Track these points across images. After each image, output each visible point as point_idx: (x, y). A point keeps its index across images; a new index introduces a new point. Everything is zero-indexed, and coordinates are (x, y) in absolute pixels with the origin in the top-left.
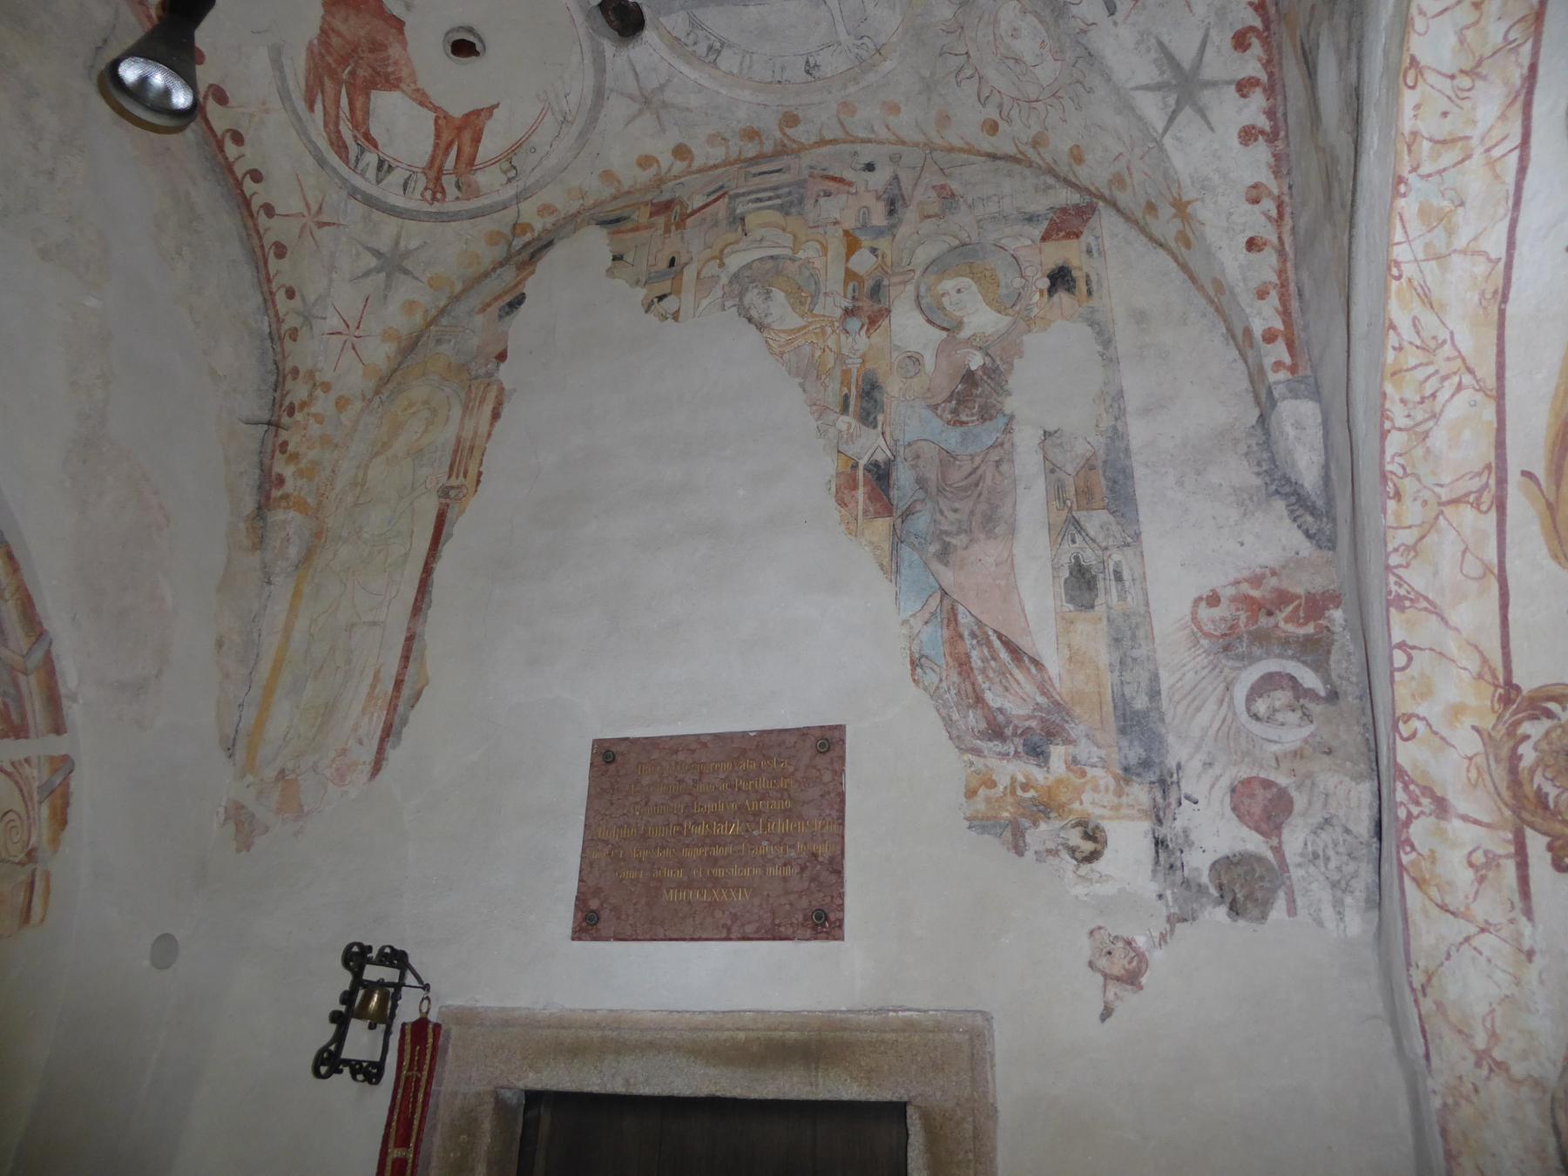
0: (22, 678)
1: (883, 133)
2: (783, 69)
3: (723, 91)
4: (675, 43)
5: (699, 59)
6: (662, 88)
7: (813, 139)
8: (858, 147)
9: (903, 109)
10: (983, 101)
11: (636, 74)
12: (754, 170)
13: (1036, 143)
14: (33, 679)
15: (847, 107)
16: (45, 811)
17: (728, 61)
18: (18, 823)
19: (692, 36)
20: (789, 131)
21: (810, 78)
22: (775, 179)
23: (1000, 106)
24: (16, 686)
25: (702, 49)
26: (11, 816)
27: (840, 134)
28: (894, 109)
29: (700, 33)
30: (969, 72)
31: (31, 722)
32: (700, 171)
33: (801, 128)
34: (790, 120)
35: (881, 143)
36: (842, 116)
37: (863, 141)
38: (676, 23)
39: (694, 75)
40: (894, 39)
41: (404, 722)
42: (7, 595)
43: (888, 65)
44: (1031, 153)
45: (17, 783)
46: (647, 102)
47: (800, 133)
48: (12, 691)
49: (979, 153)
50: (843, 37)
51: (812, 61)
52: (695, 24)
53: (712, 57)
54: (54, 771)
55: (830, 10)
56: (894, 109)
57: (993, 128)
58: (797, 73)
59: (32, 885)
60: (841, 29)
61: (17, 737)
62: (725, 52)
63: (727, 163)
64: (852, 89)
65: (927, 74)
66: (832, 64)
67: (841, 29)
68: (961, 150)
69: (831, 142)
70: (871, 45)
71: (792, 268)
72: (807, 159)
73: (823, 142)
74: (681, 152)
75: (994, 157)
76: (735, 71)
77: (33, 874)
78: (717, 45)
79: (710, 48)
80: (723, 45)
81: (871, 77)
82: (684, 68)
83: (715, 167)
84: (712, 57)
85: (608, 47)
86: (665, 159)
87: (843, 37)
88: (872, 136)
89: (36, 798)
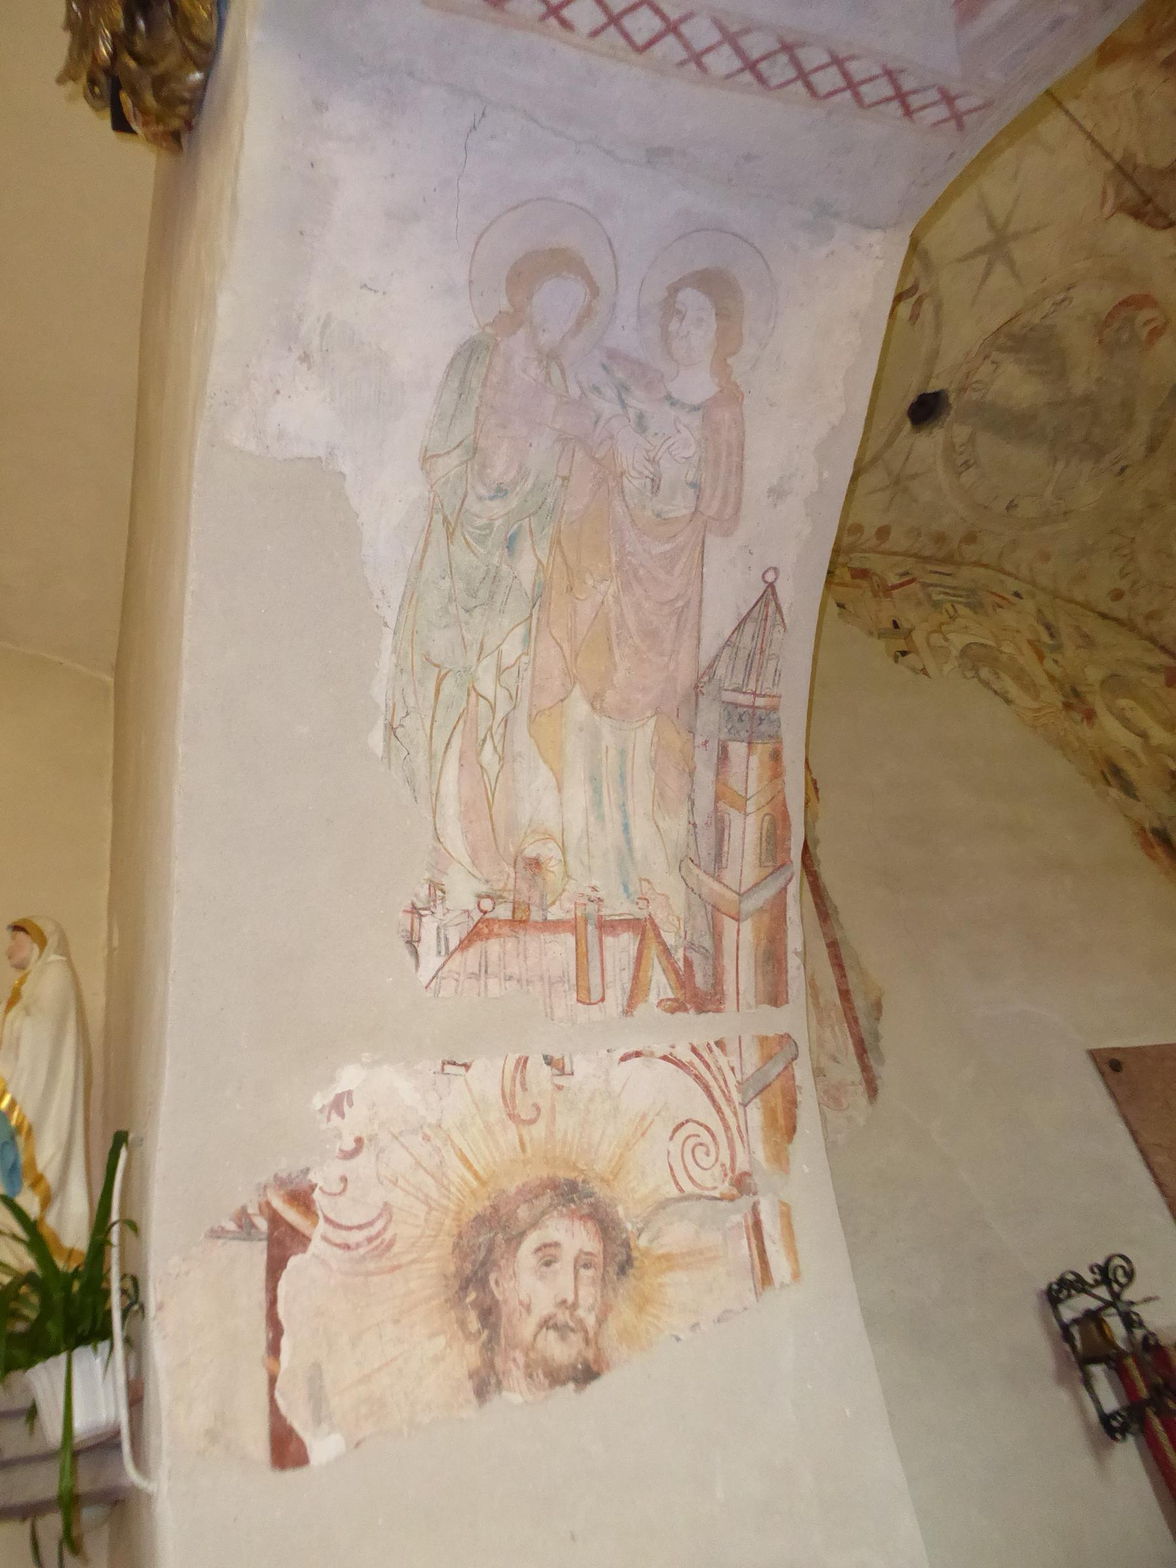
0: (729, 925)
4: (950, 447)
6: (913, 477)
7: (974, 559)
8: (1003, 577)
10: (1123, 574)
11: (907, 458)
12: (929, 567)
13: (1150, 616)
14: (747, 927)
16: (755, 1115)
17: (968, 478)
18: (706, 1137)
22: (948, 581)
23: (1134, 583)
24: (717, 935)
26: (690, 1128)
30: (1126, 551)
31: (729, 987)
32: (883, 553)
34: (971, 538)
37: (1009, 574)
38: (961, 433)
41: (877, 1037)
42: (751, 807)
44: (1140, 621)
45: (698, 1078)
46: (897, 482)
47: (970, 552)
48: (707, 942)
49: (1092, 610)
52: (971, 440)
54: (768, 1058)
56: (1045, 557)
57: (1118, 595)
59: (757, 1225)
61: (701, 1010)
63: (906, 554)
68: (1078, 603)
69: (985, 566)
71: (1004, 658)
72: (966, 572)
73: (978, 564)
74: (883, 532)
75: (1104, 616)
77: (755, 1210)
79: (966, 462)
83: (895, 554)
85: (908, 425)
86: (870, 532)
89: (736, 1097)
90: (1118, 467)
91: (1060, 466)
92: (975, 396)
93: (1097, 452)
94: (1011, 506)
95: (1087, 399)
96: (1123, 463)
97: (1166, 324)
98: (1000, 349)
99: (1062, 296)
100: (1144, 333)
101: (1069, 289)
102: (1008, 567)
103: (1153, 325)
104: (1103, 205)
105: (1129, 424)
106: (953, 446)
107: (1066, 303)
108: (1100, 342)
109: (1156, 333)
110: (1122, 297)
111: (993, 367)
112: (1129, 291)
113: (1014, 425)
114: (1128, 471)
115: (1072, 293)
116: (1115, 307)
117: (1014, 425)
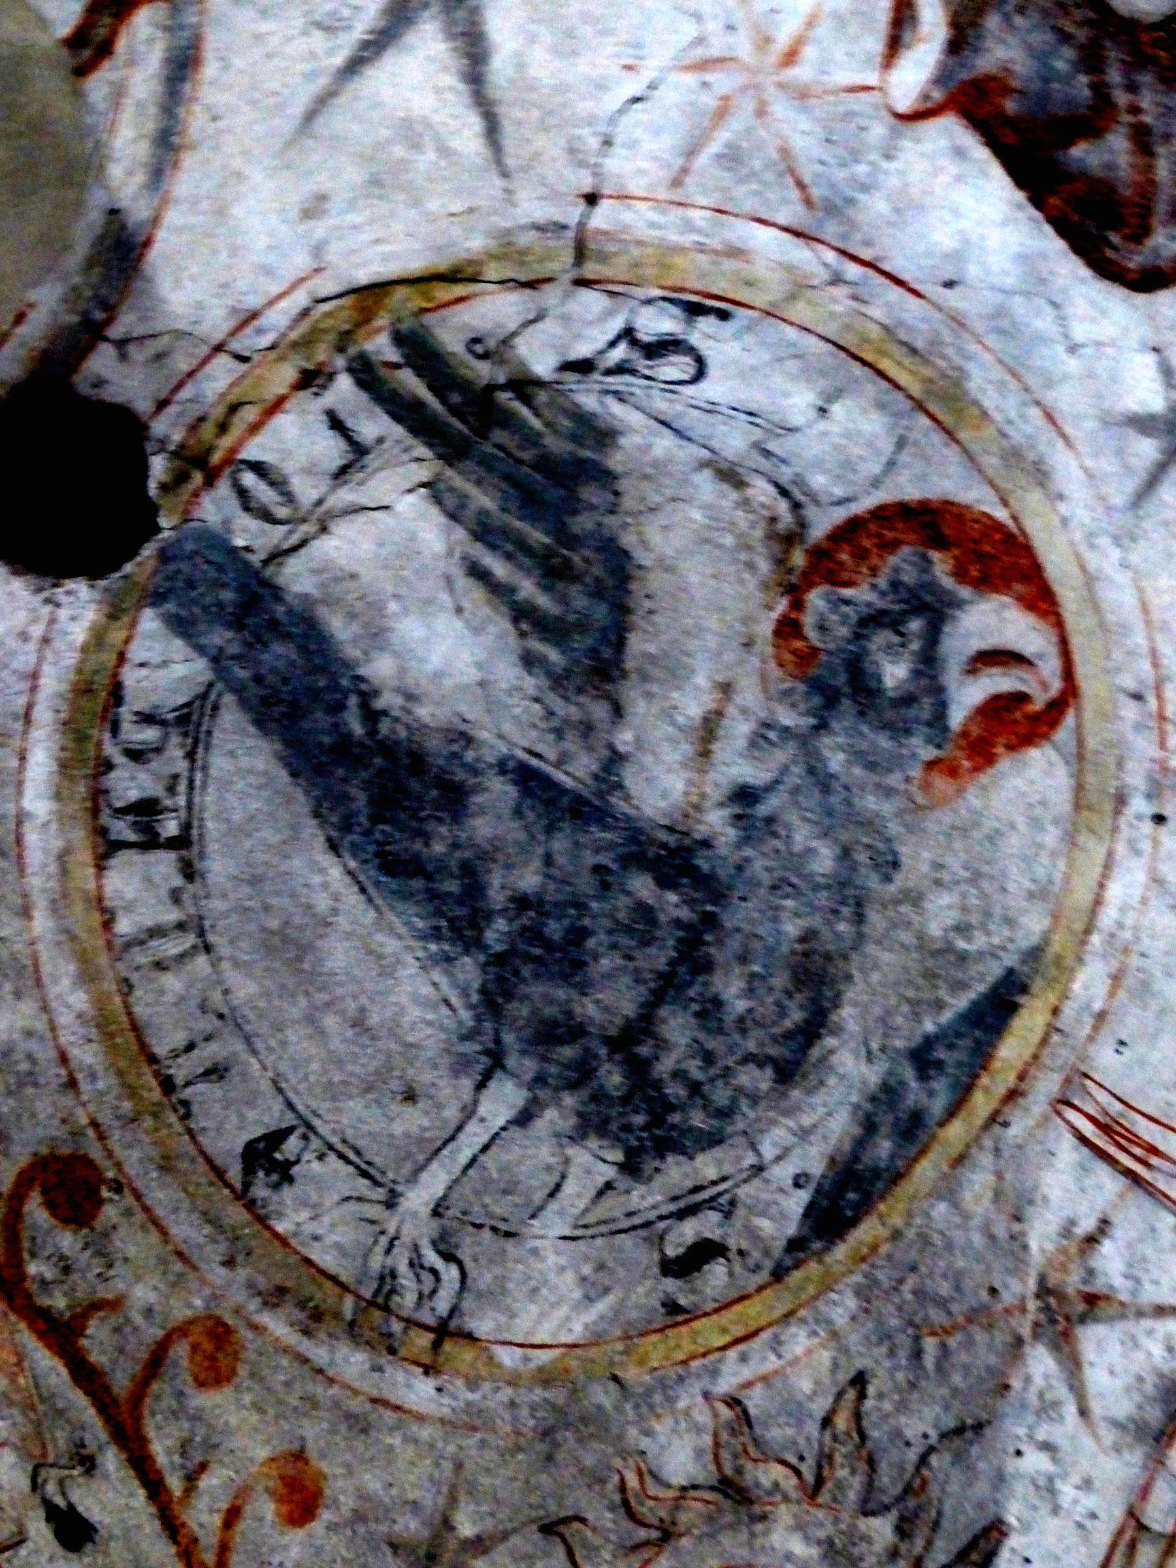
1: (203, 1517)
2: (216, 1072)
3: (42, 923)
4: (98, 697)
5: (98, 796)
8: (111, 1460)
9: (317, 1527)
15: (217, 1350)
17: (138, 887)
19: (150, 734)
20: (36, 1211)
21: (235, 1173)
25: (130, 784)
27: (121, 1382)
28: (301, 1499)
29: (175, 758)
33: (67, 1241)
35: (171, 1526)
36: (180, 1351)
39: (37, 801)
40: (507, 1357)
43: (418, 1392)
50: (419, 1198)
51: (292, 1144)
52: (190, 721)
53: (122, 829)
55: (469, 1112)
56: (301, 1499)
58: (229, 1128)
60: (435, 1182)
62: (164, 864)
64: (279, 1326)
65: (466, 1529)
66: (319, 1216)
67: (435, 1182)
70: (442, 1304)
76: (124, 926)
78: (170, 827)
79: (146, 810)
80: (181, 842)
81: (352, 1362)
82: (41, 762)
84: (122, 829)
87: (419, 1198)
88: (175, 1484)
90: (689, 1231)
91: (502, 1100)
92: (248, 533)
93: (645, 1120)
94: (266, 1157)
95: (675, 857)
96: (705, 1226)
97: (1057, 709)
98: (367, 375)
99: (658, 323)
100: (967, 696)
101: (694, 310)
102: (162, 1449)
103: (999, 682)
104: (895, 45)
105: (793, 1063)
106: (116, 694)
107: (674, 368)
108: (788, 628)
109: (1015, 724)
110: (907, 487)
111: (329, 449)
112: (943, 479)
113: (380, 785)
114: (716, 1275)
115: (703, 333)
116: (881, 514)
117: (380, 785)
